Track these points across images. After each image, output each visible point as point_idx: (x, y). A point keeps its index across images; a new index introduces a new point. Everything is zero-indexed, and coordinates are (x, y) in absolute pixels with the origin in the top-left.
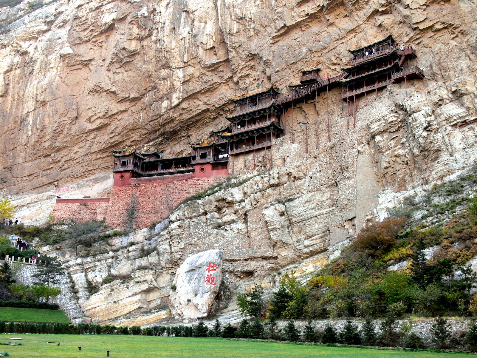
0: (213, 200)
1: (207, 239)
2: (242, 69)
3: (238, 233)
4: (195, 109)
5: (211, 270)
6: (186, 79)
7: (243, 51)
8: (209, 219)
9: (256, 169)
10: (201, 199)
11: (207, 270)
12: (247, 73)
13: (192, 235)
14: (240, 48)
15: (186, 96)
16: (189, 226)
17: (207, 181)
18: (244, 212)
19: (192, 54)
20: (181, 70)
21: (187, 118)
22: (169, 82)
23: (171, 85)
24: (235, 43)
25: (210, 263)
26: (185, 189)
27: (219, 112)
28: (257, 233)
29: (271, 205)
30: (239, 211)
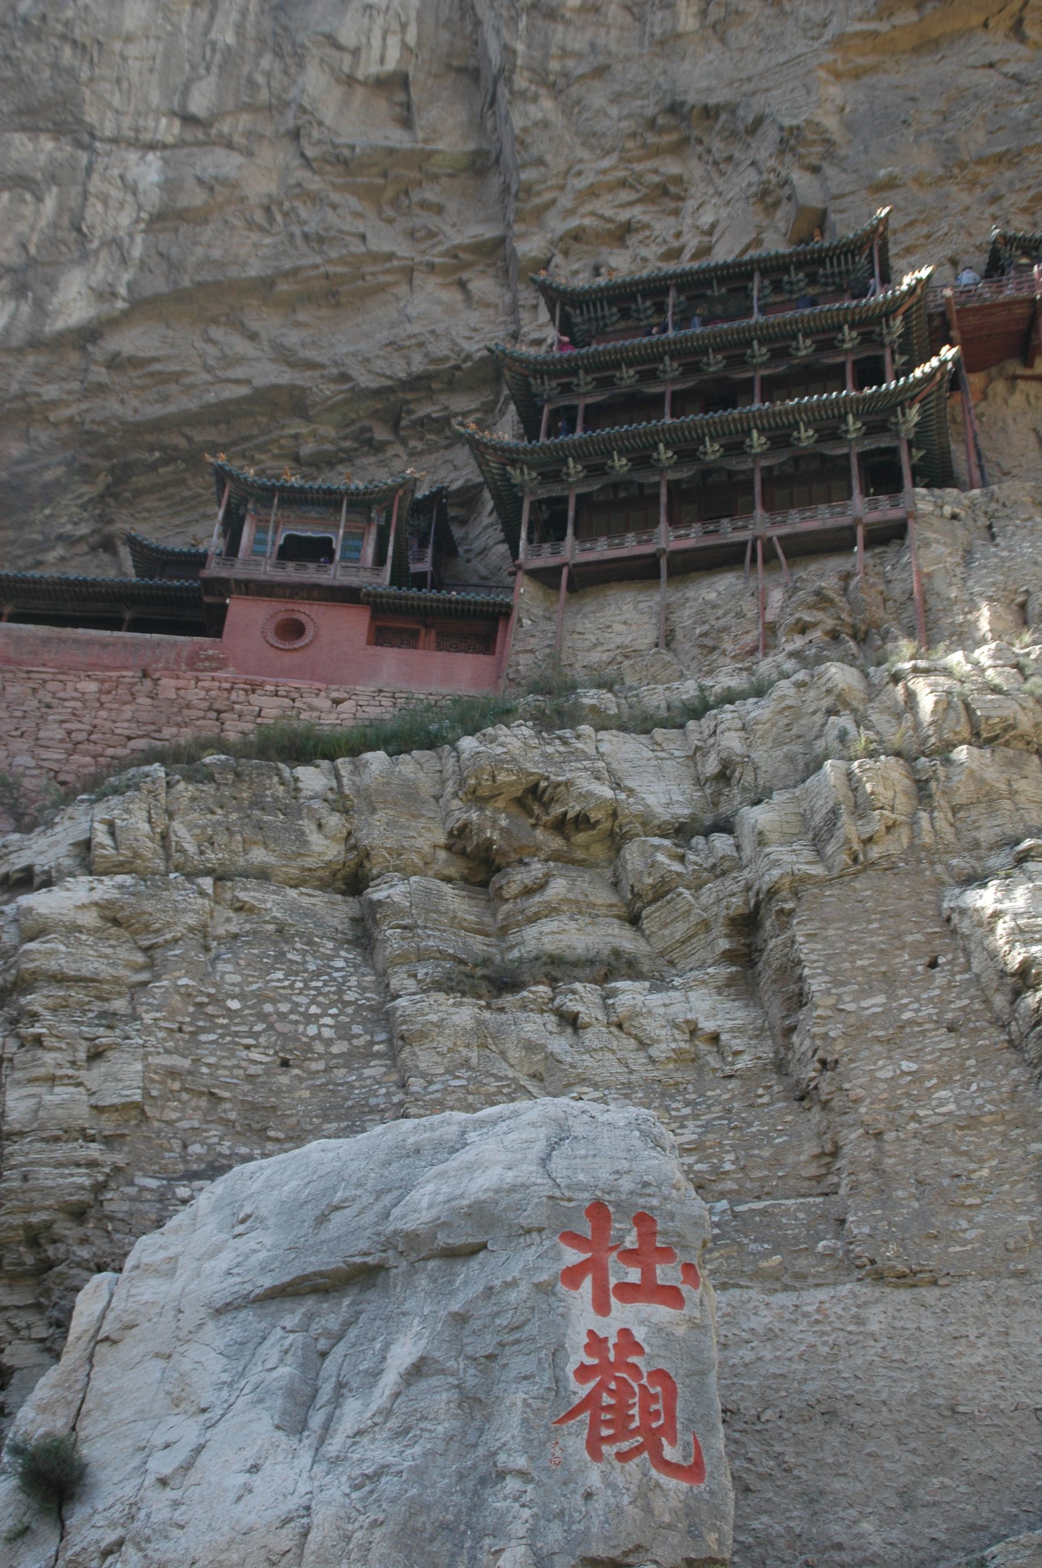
0: (426, 785)
1: (375, 1070)
2: (592, 192)
3: (679, 1057)
4: (207, 377)
5: (627, 1292)
6: (183, 201)
7: (616, 98)
8: (399, 912)
9: (790, 647)
10: (325, 764)
11: (572, 1276)
12: (624, 215)
13: (231, 1013)
14: (597, 84)
15: (157, 284)
16: (202, 930)
17: (323, 703)
18: (737, 904)
19: (251, 83)
20: (151, 157)
21: (138, 417)
22: (49, 204)
23: (65, 221)
24: (565, 53)
25: (598, 1211)
26: (123, 728)
27: (367, 423)
28: (906, 1066)
29: (1022, 858)
30: (686, 893)
